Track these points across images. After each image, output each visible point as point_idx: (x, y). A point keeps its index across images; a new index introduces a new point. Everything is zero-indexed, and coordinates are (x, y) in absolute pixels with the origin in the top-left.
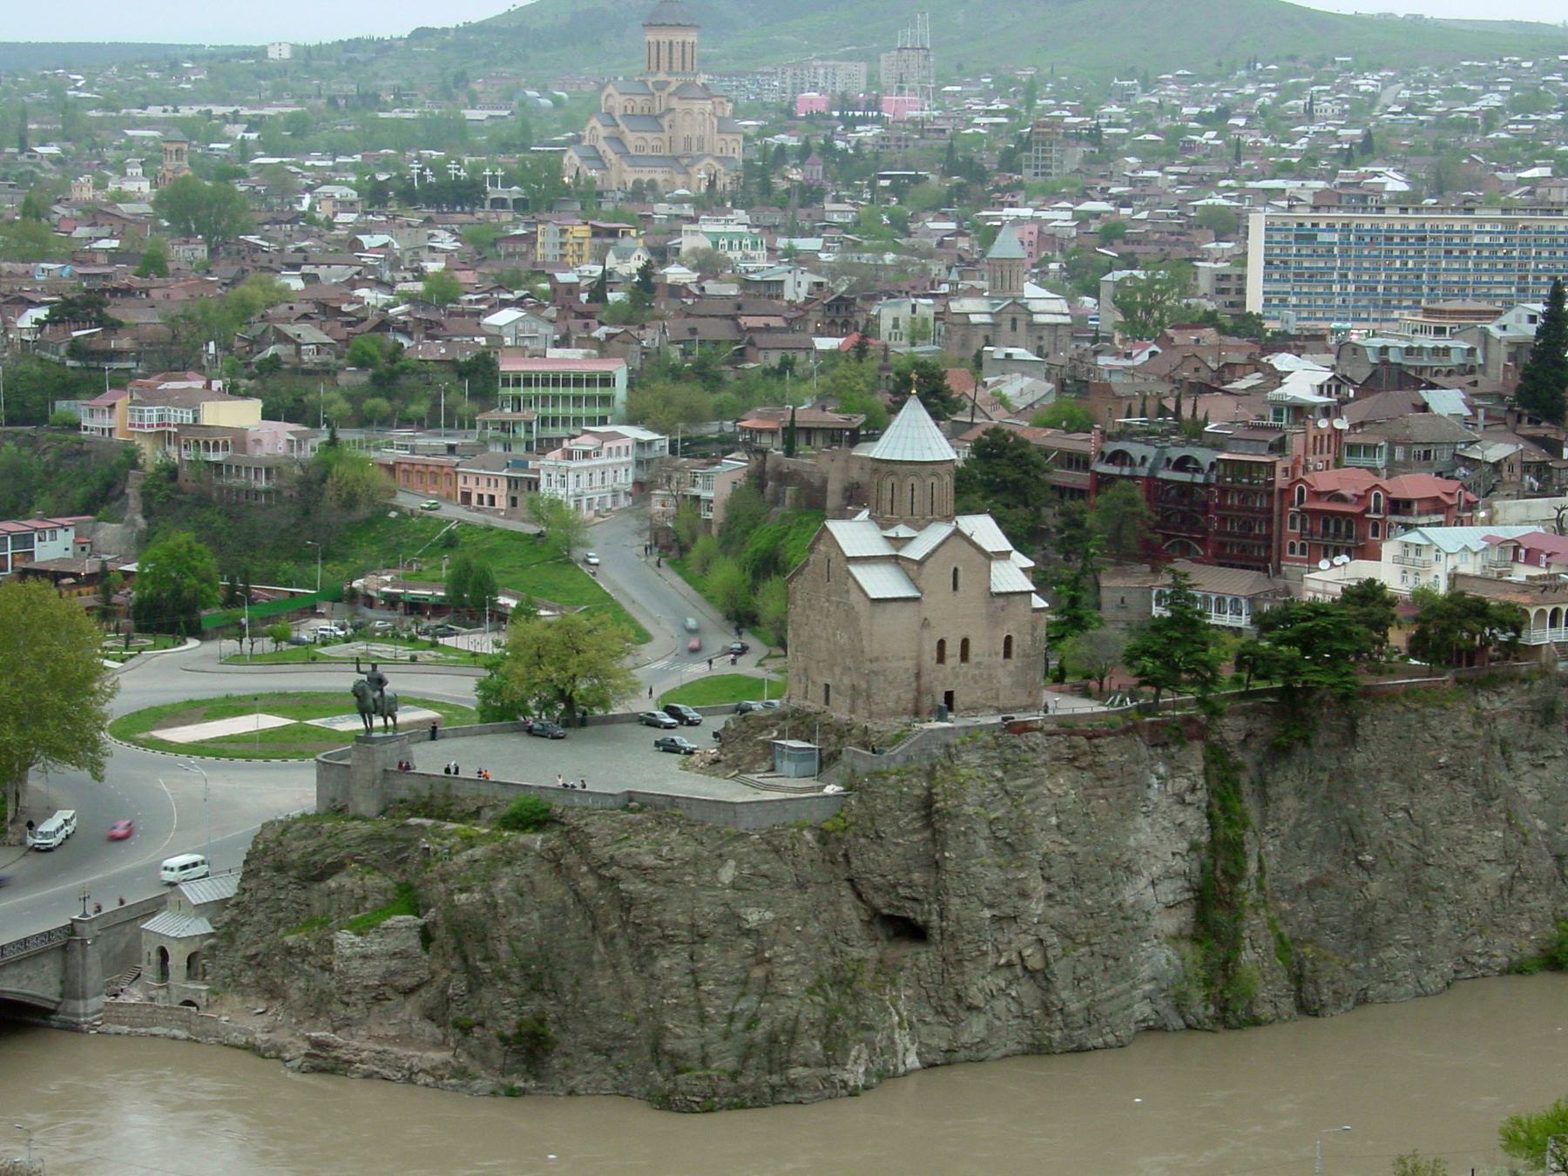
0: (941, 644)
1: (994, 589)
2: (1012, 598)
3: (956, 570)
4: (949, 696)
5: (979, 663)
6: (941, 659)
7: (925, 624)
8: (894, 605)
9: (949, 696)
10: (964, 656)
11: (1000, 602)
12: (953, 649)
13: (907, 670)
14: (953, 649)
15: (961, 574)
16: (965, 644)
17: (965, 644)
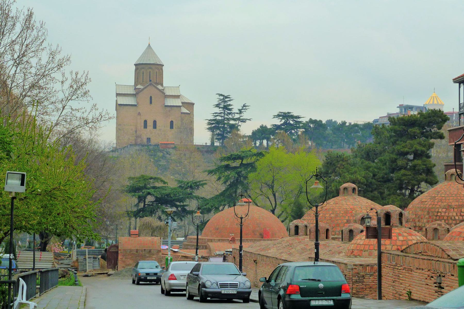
0: (145, 122)
1: (166, 104)
2: (173, 108)
3: (151, 97)
4: (149, 139)
5: (160, 130)
6: (145, 126)
7: (139, 114)
8: (127, 107)
9: (149, 139)
10: (155, 126)
11: (168, 109)
12: (150, 124)
13: (132, 129)
14: (150, 124)
15: (153, 98)
16: (155, 122)
17: (155, 122)
